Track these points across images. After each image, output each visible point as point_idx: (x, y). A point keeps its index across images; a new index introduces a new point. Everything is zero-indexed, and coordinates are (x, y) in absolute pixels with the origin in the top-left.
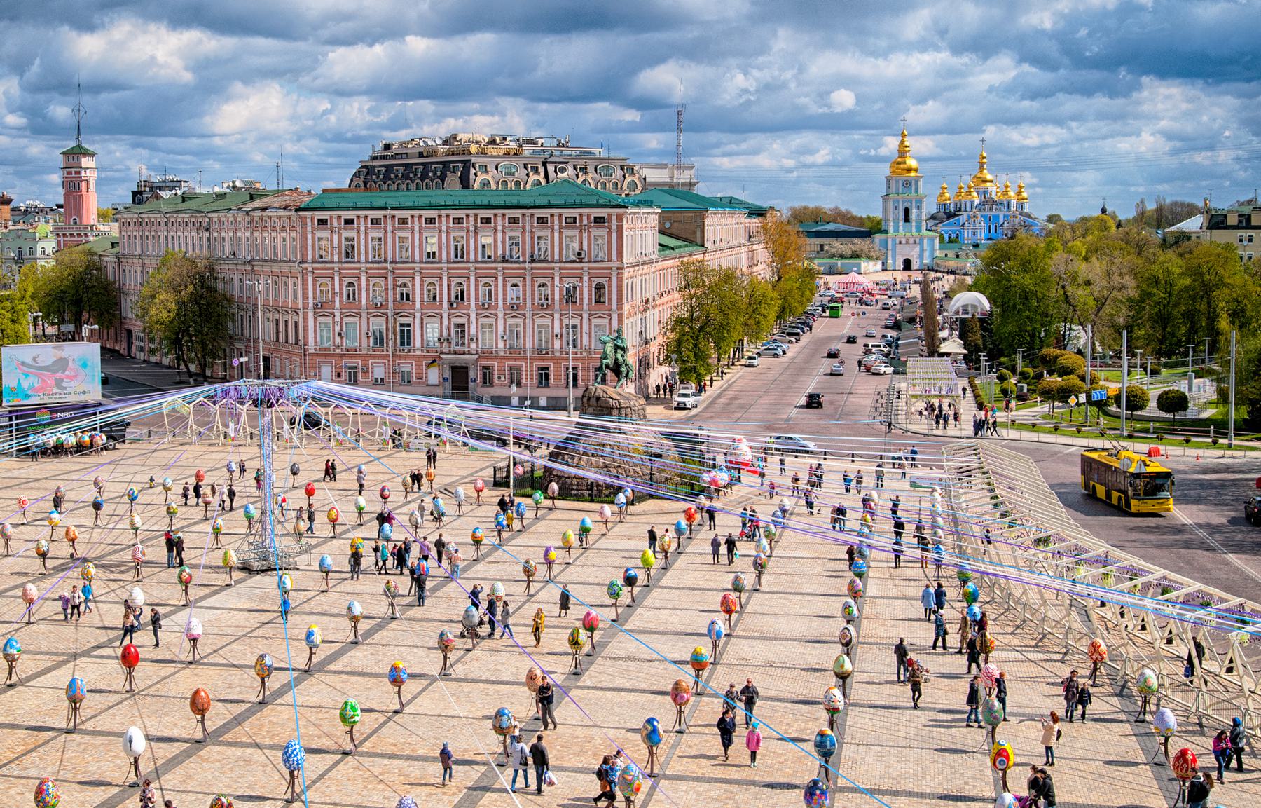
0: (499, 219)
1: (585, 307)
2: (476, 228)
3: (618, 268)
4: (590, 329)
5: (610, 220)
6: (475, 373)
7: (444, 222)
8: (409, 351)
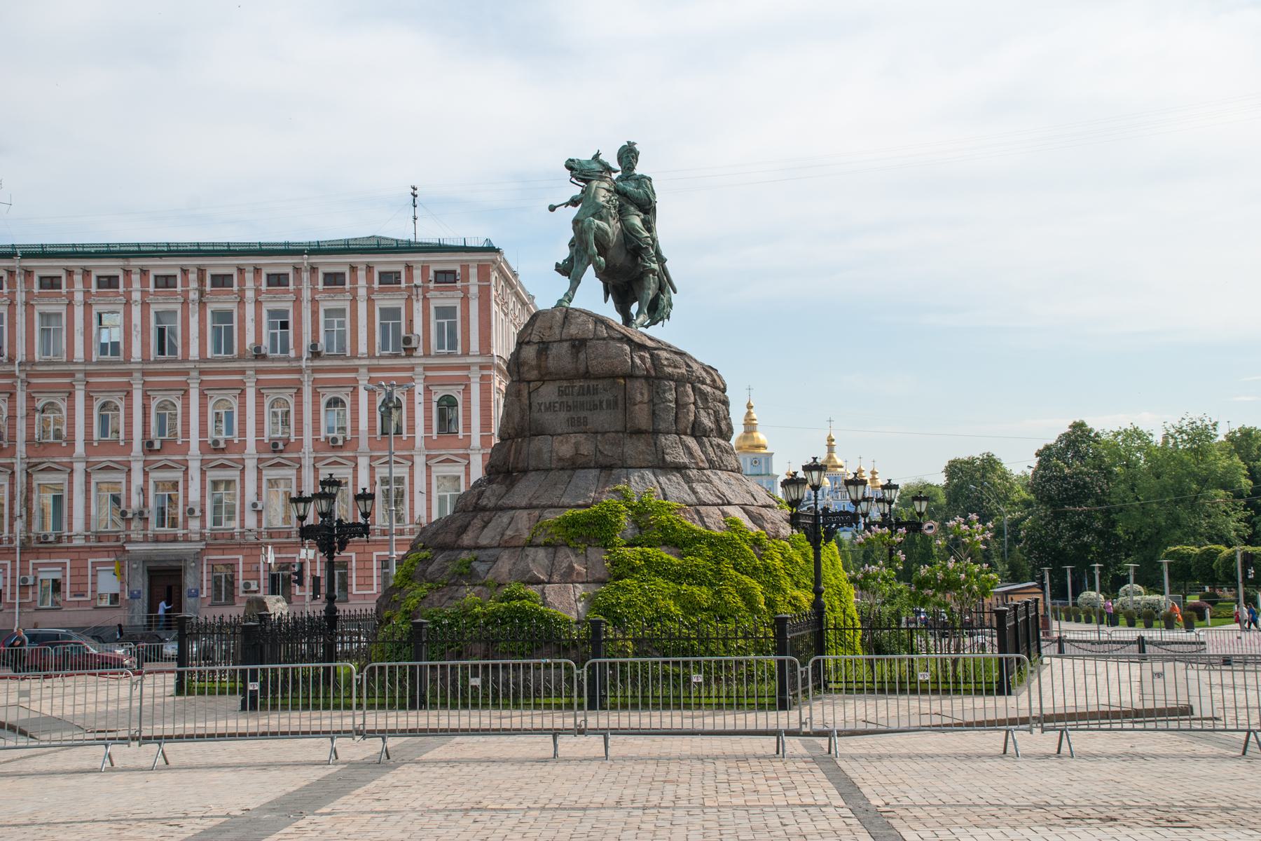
0: (249, 276)
1: (419, 442)
2: (202, 293)
3: (482, 367)
4: (429, 484)
5: (466, 277)
6: (198, 581)
7: (136, 285)
8: (59, 539)
